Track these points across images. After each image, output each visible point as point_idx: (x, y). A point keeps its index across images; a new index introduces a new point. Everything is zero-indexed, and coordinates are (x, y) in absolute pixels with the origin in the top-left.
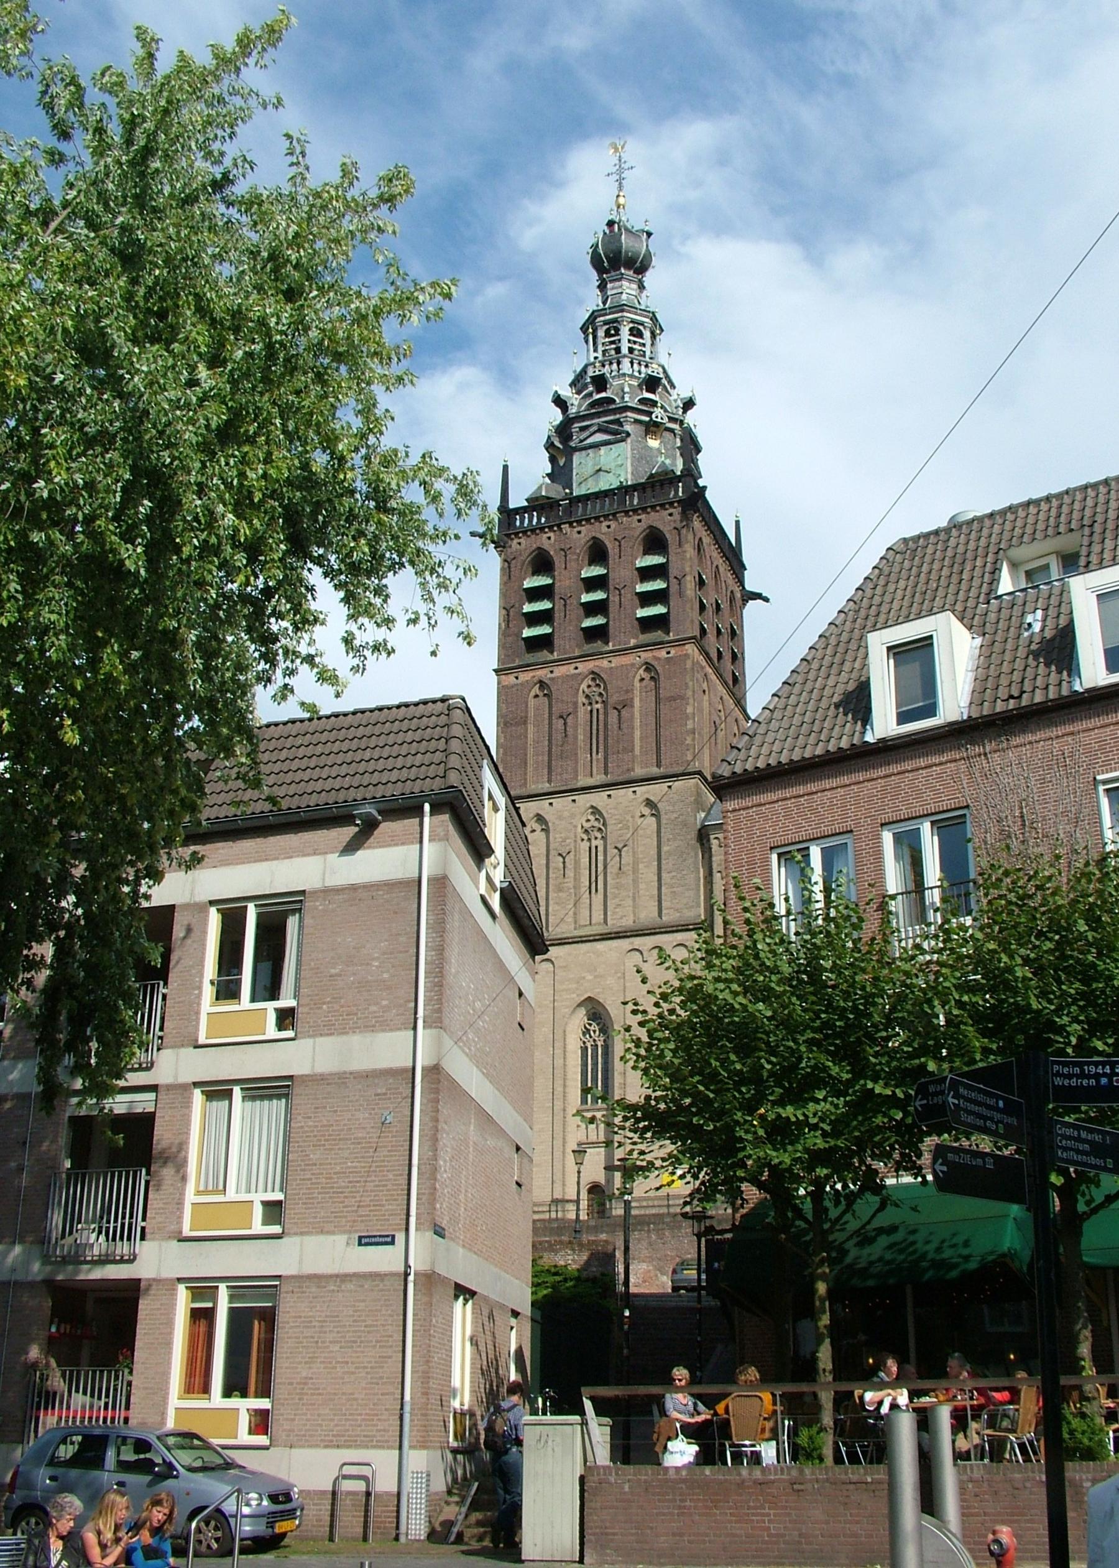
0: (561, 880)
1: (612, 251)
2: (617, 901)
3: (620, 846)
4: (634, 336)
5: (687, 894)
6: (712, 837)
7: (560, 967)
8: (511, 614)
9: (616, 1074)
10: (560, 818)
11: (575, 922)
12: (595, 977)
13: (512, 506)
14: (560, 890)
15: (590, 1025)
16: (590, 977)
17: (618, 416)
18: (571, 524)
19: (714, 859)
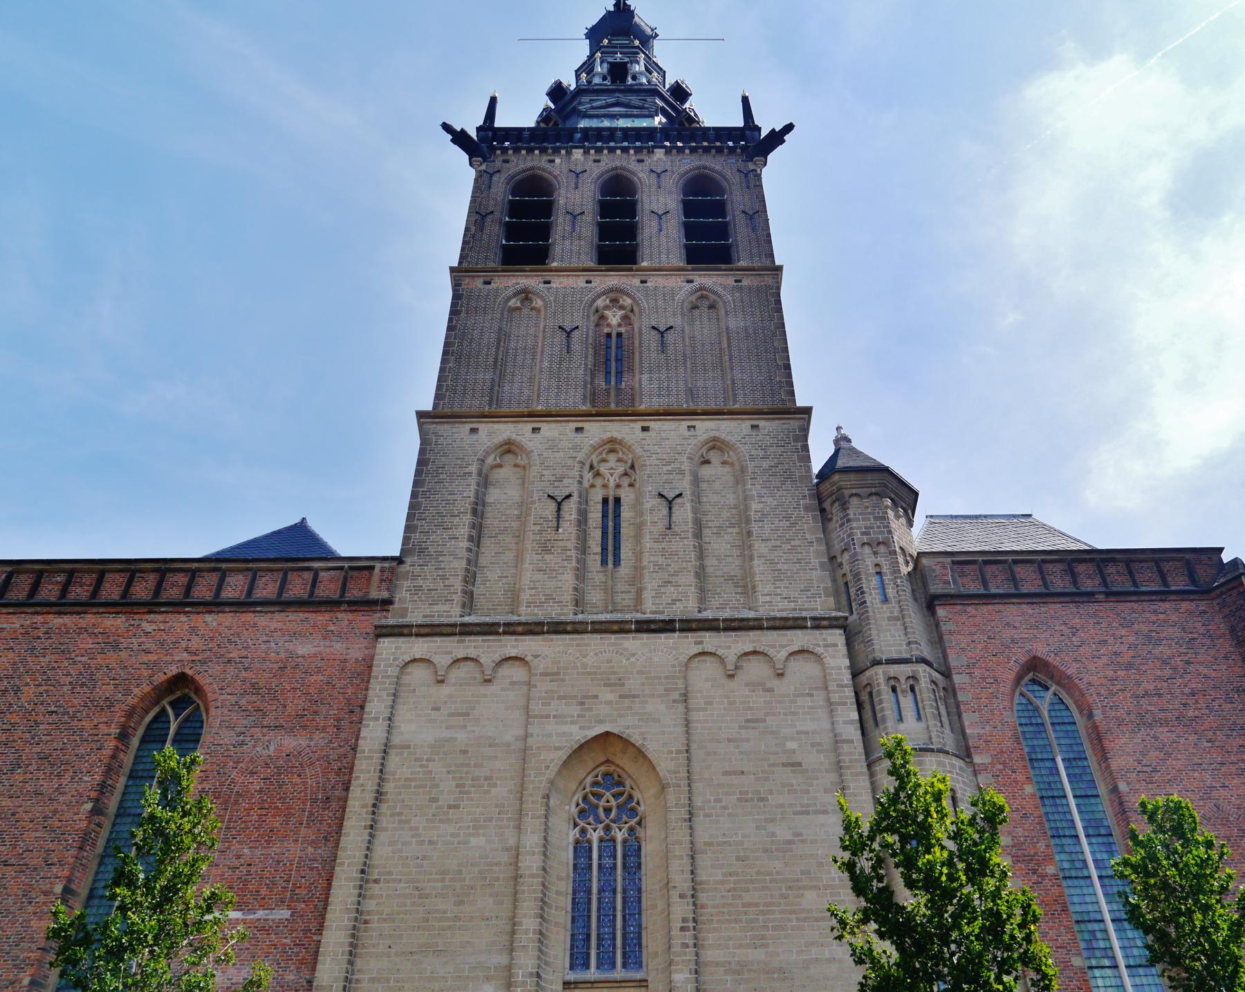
3: (670, 495)
12: (621, 697)
14: (545, 548)
16: (607, 695)
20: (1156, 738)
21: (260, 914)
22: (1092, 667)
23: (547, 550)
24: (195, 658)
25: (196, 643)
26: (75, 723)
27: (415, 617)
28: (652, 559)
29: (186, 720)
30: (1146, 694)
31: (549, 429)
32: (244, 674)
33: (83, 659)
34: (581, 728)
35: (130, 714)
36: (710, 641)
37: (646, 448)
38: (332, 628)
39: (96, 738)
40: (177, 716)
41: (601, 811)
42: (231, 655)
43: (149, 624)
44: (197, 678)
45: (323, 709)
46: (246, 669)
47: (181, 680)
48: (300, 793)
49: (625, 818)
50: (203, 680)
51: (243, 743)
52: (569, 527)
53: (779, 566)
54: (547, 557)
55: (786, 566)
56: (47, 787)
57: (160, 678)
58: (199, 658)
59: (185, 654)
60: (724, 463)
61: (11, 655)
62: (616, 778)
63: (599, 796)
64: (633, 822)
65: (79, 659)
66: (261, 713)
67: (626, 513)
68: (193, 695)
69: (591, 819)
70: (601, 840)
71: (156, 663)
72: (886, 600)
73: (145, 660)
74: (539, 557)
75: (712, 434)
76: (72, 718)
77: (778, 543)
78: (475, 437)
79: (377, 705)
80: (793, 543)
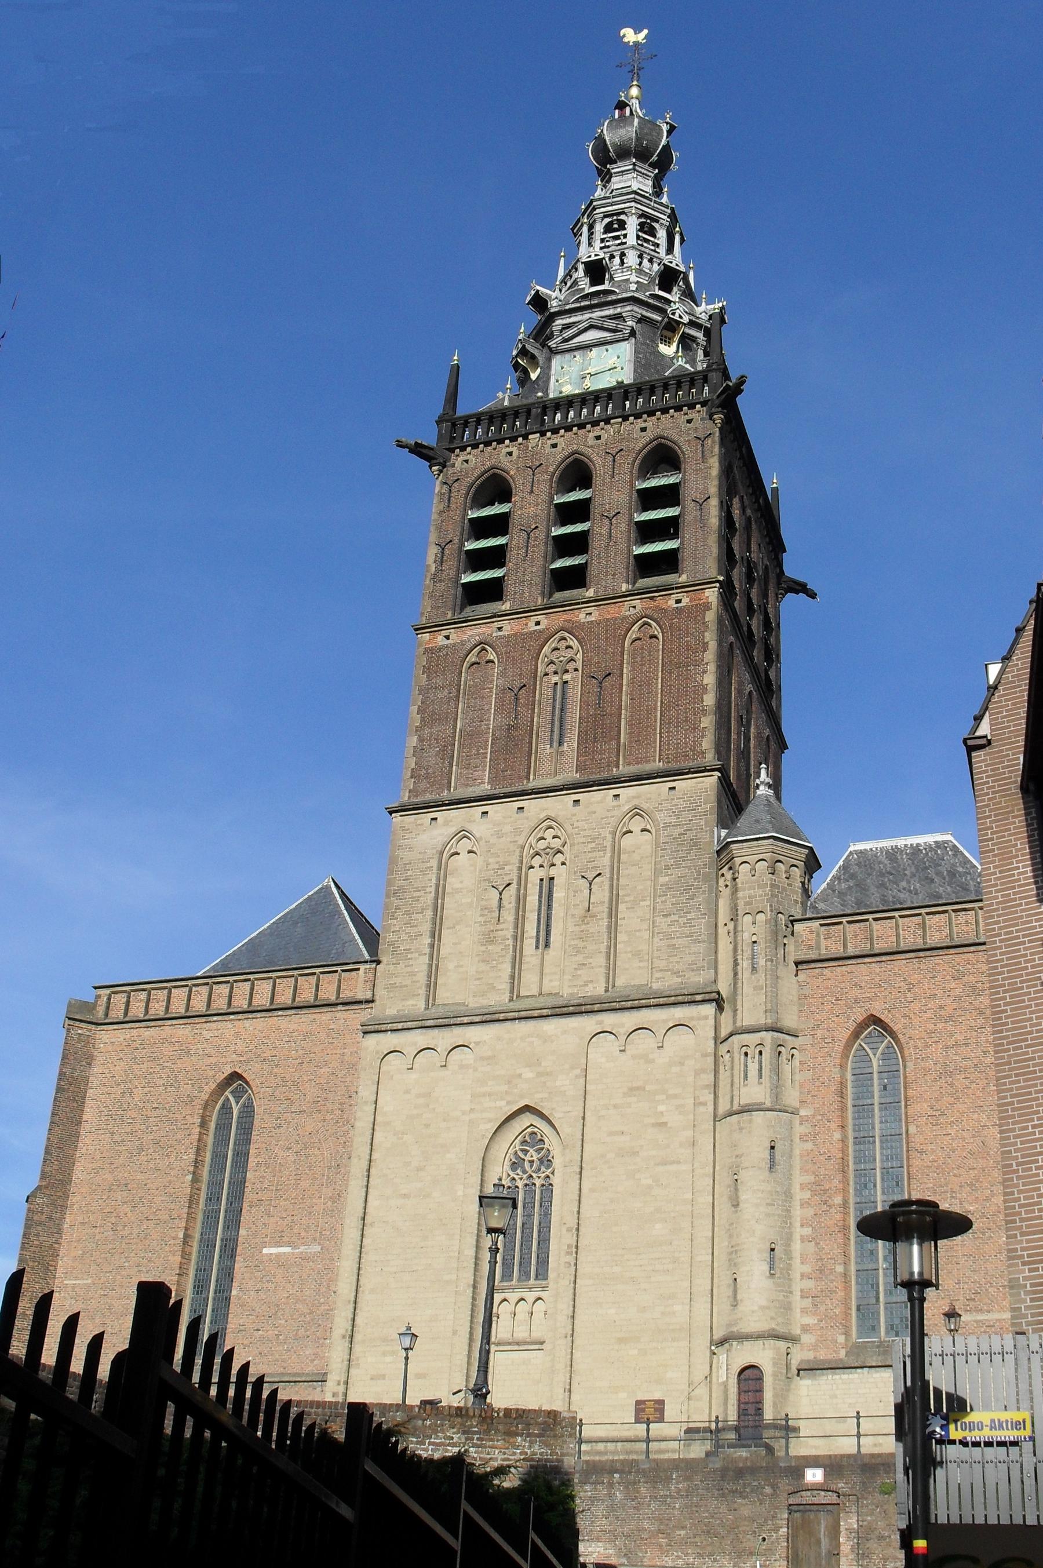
2: (580, 958)
4: (645, 233)
5: (694, 949)
6: (738, 860)
8: (447, 552)
11: (512, 992)
12: (539, 1074)
15: (525, 1152)
16: (530, 1075)
17: (619, 310)
20: (952, 1085)
21: (302, 1248)
22: (916, 1021)
23: (490, 942)
25: (241, 1046)
27: (391, 1011)
28: (573, 943)
29: (244, 1106)
30: (957, 1044)
32: (276, 1070)
34: (508, 1103)
35: (205, 1107)
36: (609, 1020)
39: (186, 1127)
40: (237, 1103)
41: (527, 1165)
45: (331, 1096)
46: (277, 1066)
47: (235, 1076)
51: (280, 1126)
52: (508, 916)
53: (674, 942)
55: (680, 941)
56: (162, 1164)
57: (221, 1077)
59: (234, 1056)
61: (122, 1064)
62: (539, 1137)
63: (525, 1152)
65: (166, 1064)
66: (289, 1101)
67: (558, 894)
69: (519, 1171)
72: (754, 969)
74: (483, 948)
75: (636, 802)
77: (676, 917)
79: (366, 1092)
80: (692, 915)
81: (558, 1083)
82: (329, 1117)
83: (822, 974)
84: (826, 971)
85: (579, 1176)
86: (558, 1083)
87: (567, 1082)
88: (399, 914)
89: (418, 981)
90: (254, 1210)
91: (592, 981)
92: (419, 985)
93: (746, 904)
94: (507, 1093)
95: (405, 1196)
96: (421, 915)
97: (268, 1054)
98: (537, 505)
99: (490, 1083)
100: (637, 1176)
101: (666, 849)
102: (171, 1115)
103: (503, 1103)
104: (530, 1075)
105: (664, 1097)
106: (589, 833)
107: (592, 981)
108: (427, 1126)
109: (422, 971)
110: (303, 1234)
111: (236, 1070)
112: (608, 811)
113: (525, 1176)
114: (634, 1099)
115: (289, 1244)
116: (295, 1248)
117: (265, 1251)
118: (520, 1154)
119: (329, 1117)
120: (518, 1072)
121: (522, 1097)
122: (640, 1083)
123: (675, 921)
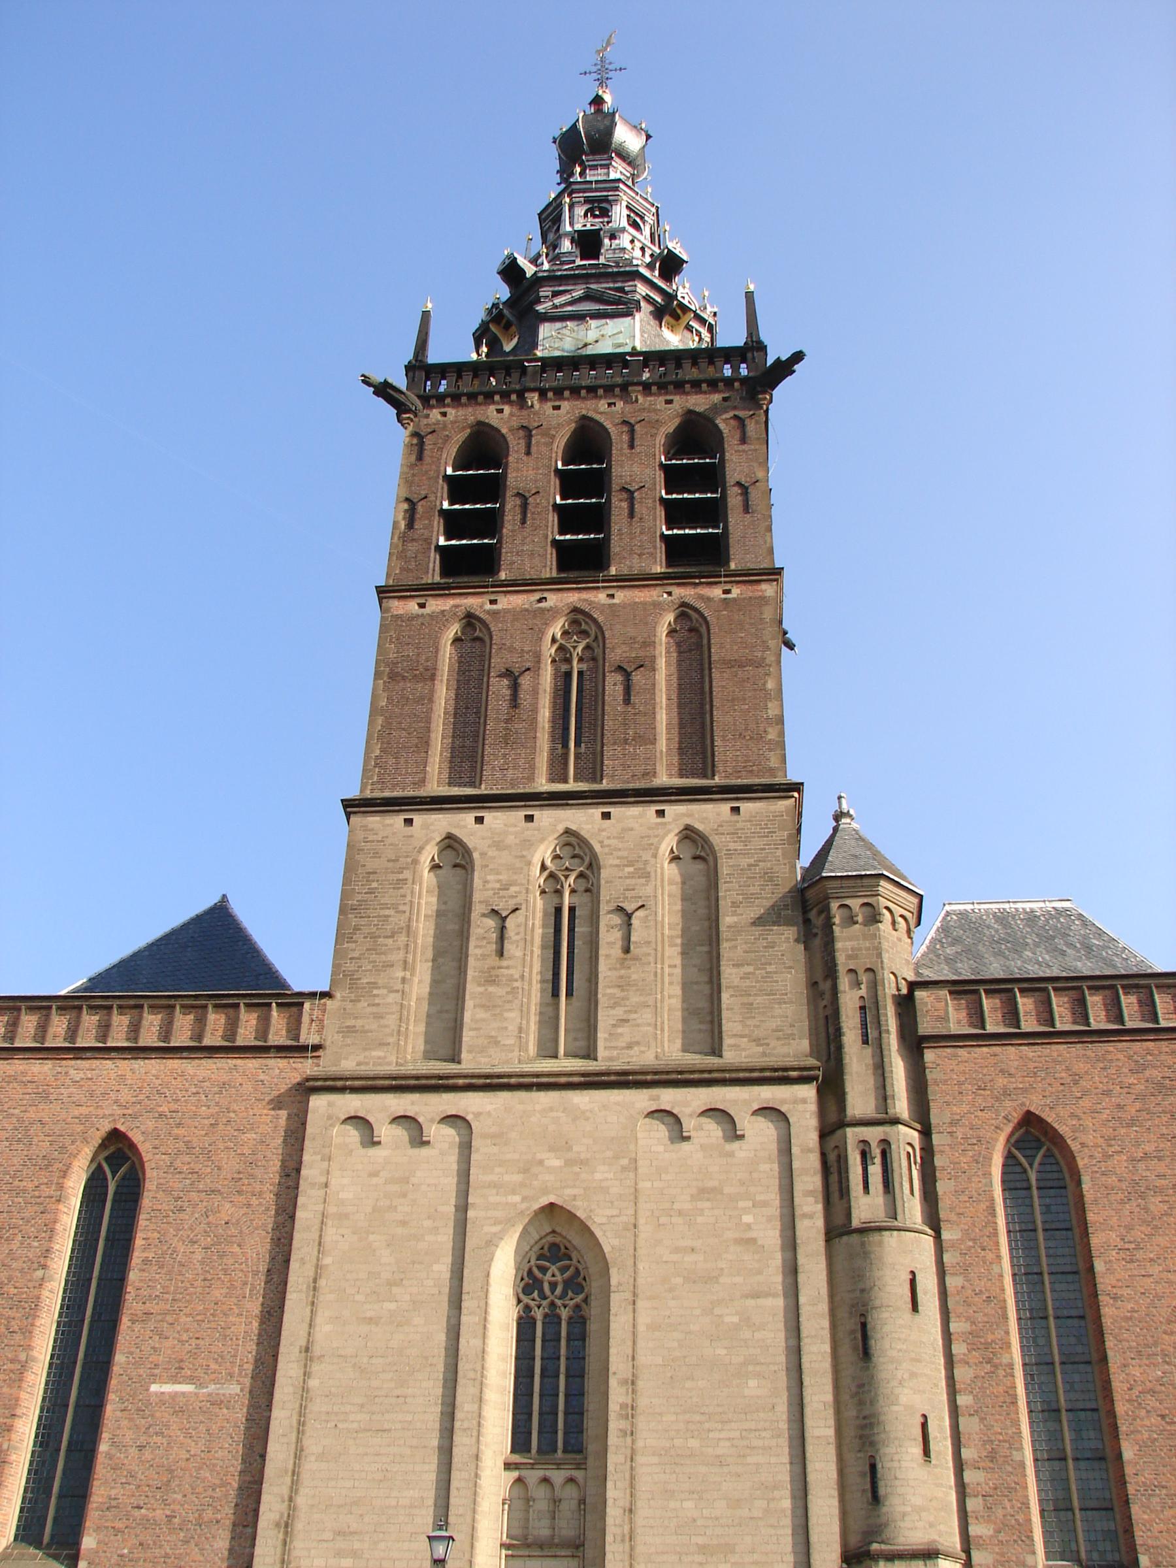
0: (494, 960)
1: (599, 131)
2: (619, 1012)
3: (630, 908)
7: (485, 1136)
9: (613, 1382)
10: (499, 845)
12: (569, 1163)
13: (435, 356)
15: (544, 1270)
16: (557, 1163)
18: (543, 394)
19: (839, 945)
21: (212, 1388)
24: (126, 1112)
25: (125, 1096)
26: (16, 1183)
27: (350, 1065)
28: (609, 991)
29: (123, 1178)
31: (495, 819)
33: (16, 1111)
37: (606, 842)
38: (262, 1077)
39: (38, 1200)
40: (114, 1174)
42: (161, 1109)
43: (77, 1069)
44: (130, 1134)
46: (179, 1125)
48: (241, 1264)
49: (570, 1294)
50: (136, 1137)
51: (181, 1210)
54: (491, 989)
55: (759, 999)
58: (130, 1112)
60: (695, 858)
63: (544, 1270)
64: (579, 1298)
65: (12, 1111)
66: (195, 1176)
68: (127, 1151)
69: (536, 1294)
70: (546, 1316)
71: (88, 1117)
73: (76, 1113)
74: (481, 989)
76: (13, 1177)
77: (750, 969)
78: (409, 830)
80: (769, 969)
81: (598, 1176)
82: (254, 1201)
83: (956, 1056)
84: (961, 1051)
85: (631, 1307)
86: (598, 1176)
87: (611, 1176)
88: (358, 937)
89: (386, 1026)
90: (137, 1327)
91: (638, 1043)
92: (387, 1030)
93: (849, 957)
94: (522, 1185)
95: (370, 1320)
96: (390, 941)
97: (164, 1108)
98: (538, 469)
99: (497, 1170)
100: (717, 1311)
101: (732, 882)
102: (16, 1183)
103: (517, 1198)
104: (557, 1163)
105: (750, 1204)
106: (625, 854)
107: (638, 1043)
108: (404, 1223)
109: (393, 1013)
110: (213, 1366)
111: (118, 1127)
112: (649, 828)
113: (545, 1303)
114: (708, 1204)
115: (190, 1380)
116: (201, 1386)
117: (154, 1388)
118: (536, 1271)
119: (254, 1201)
120: (539, 1156)
121: (545, 1191)
122: (716, 1183)
123: (749, 973)
